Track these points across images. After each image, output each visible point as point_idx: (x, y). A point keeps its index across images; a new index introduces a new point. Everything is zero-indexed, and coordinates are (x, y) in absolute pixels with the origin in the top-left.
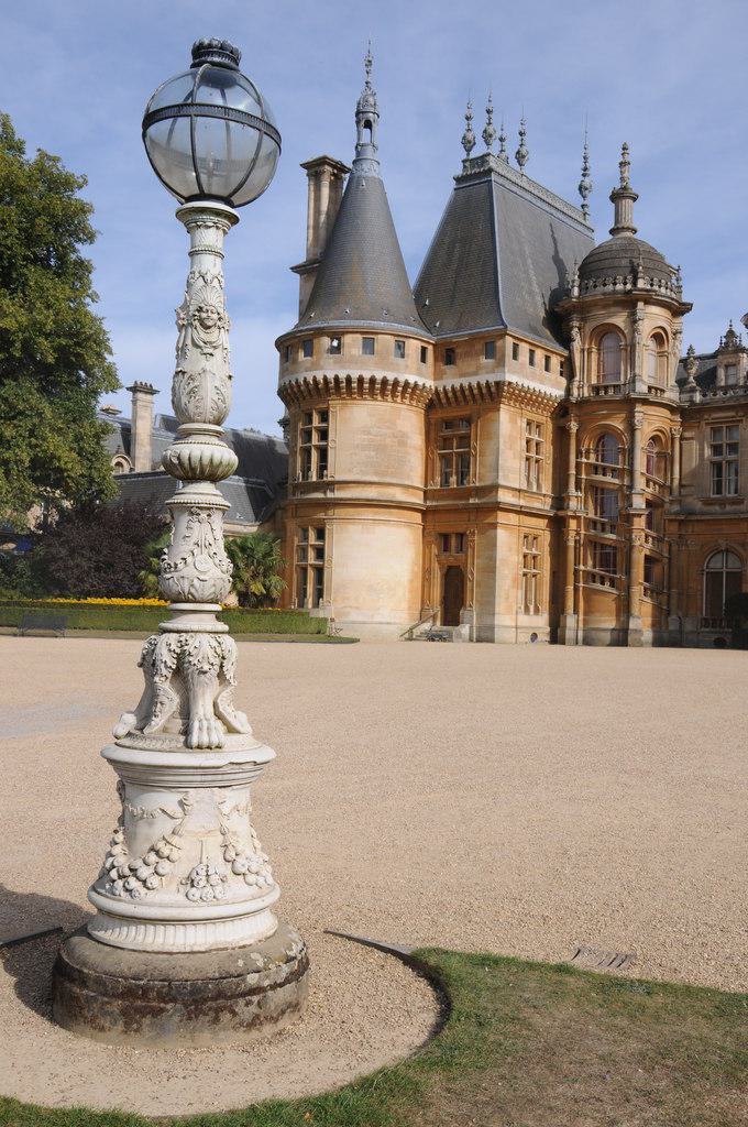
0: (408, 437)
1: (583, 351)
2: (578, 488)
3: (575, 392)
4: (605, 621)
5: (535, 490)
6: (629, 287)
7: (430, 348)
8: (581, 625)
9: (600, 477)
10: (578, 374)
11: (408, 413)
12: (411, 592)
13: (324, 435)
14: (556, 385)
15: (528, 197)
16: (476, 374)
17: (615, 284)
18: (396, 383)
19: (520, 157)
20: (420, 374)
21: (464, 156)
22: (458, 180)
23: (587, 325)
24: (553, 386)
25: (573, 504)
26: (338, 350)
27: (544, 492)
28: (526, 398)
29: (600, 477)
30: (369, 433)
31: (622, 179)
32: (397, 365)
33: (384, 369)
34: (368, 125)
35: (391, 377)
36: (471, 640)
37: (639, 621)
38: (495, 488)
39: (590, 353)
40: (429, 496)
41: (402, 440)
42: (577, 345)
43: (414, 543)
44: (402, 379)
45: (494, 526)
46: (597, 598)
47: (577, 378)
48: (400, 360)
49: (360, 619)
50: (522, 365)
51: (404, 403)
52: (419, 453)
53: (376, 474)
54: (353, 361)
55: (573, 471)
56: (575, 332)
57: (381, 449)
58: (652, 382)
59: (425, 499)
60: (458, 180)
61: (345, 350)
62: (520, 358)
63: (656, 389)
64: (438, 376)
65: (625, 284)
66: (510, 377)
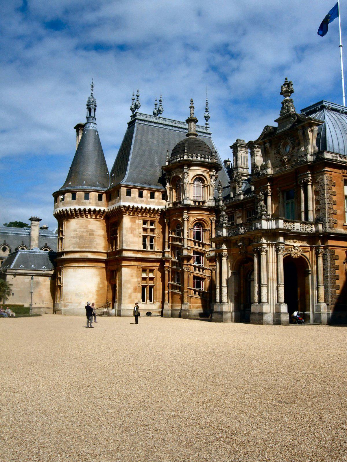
0: (94, 231)
2: (169, 247)
4: (177, 306)
5: (149, 249)
7: (104, 196)
8: (170, 308)
9: (175, 243)
10: (169, 198)
11: (95, 222)
12: (97, 295)
14: (160, 204)
15: (162, 126)
16: (115, 203)
17: (177, 159)
18: (85, 210)
20: (97, 205)
21: (131, 114)
24: (156, 205)
25: (167, 255)
26: (63, 199)
27: (156, 250)
29: (175, 243)
30: (76, 231)
32: (85, 203)
33: (79, 205)
35: (82, 208)
36: (115, 316)
37: (187, 306)
38: (122, 250)
40: (109, 255)
41: (91, 233)
43: (99, 275)
44: (87, 208)
45: (121, 267)
46: (175, 296)
47: (168, 200)
48: (87, 201)
49: (73, 307)
50: (135, 198)
51: (91, 218)
52: (102, 238)
53: (79, 247)
54: (69, 203)
57: (81, 237)
58: (199, 199)
59: (107, 256)
61: (65, 199)
62: (132, 195)
63: (199, 202)
64: (107, 206)
66: (122, 203)
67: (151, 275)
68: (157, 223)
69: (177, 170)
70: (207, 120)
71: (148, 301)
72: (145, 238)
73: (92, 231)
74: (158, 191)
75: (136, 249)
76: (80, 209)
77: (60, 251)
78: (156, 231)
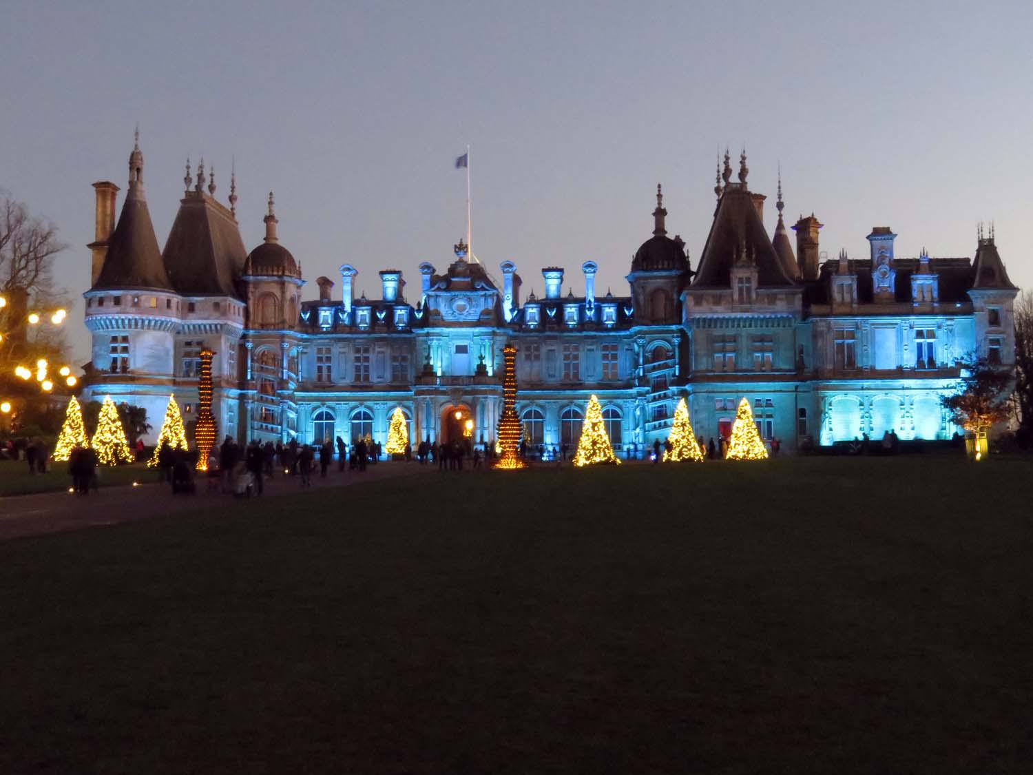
1: (254, 304)
6: (280, 273)
13: (125, 350)
16: (208, 319)
17: (273, 271)
19: (212, 188)
20: (177, 317)
22: (182, 201)
23: (257, 291)
28: (230, 332)
31: (270, 211)
34: (138, 170)
39: (258, 306)
42: (251, 302)
56: (250, 295)
60: (182, 201)
65: (278, 271)
66: (229, 322)
70: (232, 204)
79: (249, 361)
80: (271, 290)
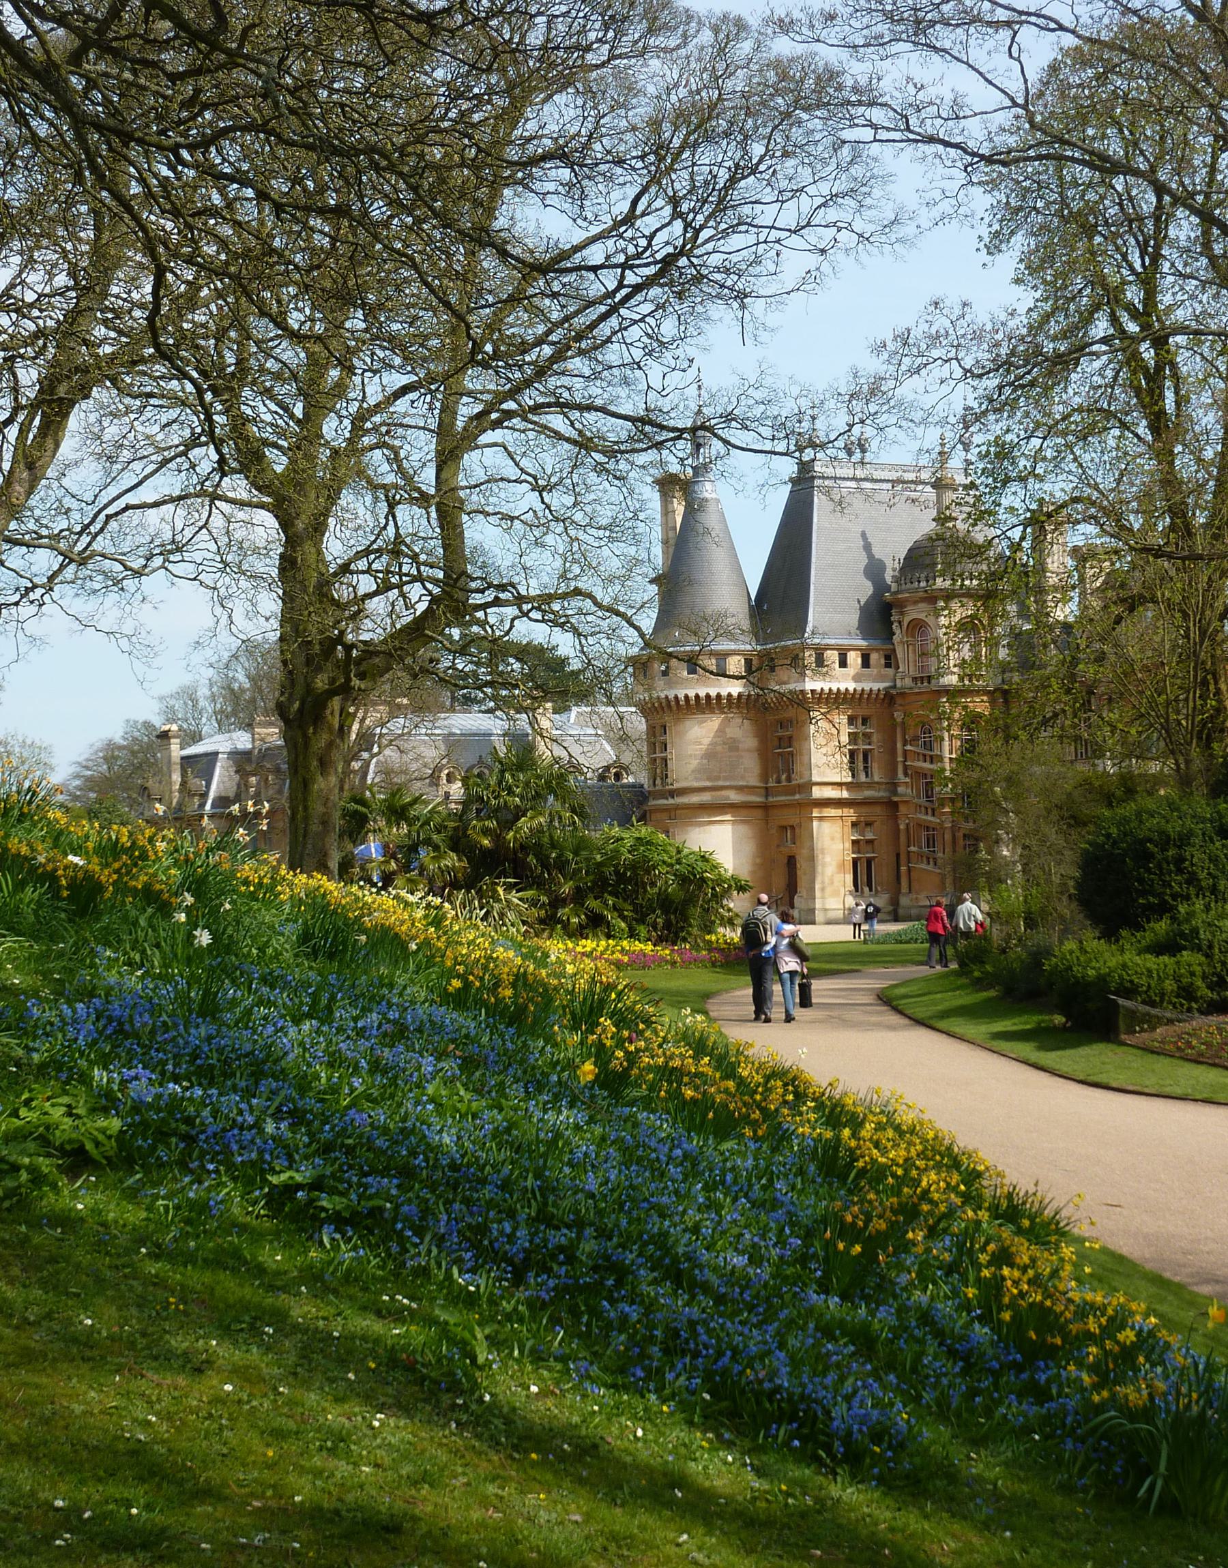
2: (906, 774)
3: (899, 683)
9: (920, 764)
14: (880, 678)
27: (876, 779)
29: (920, 764)
41: (733, 746)
55: (900, 759)
67: (870, 836)
68: (874, 721)
69: (921, 605)
71: (866, 889)
72: (852, 754)
73: (734, 740)
74: (877, 650)
75: (838, 780)
76: (708, 696)
77: (659, 787)
78: (875, 738)
79: (899, 745)
80: (922, 616)
